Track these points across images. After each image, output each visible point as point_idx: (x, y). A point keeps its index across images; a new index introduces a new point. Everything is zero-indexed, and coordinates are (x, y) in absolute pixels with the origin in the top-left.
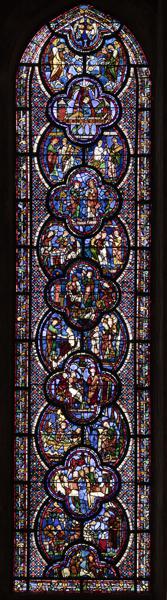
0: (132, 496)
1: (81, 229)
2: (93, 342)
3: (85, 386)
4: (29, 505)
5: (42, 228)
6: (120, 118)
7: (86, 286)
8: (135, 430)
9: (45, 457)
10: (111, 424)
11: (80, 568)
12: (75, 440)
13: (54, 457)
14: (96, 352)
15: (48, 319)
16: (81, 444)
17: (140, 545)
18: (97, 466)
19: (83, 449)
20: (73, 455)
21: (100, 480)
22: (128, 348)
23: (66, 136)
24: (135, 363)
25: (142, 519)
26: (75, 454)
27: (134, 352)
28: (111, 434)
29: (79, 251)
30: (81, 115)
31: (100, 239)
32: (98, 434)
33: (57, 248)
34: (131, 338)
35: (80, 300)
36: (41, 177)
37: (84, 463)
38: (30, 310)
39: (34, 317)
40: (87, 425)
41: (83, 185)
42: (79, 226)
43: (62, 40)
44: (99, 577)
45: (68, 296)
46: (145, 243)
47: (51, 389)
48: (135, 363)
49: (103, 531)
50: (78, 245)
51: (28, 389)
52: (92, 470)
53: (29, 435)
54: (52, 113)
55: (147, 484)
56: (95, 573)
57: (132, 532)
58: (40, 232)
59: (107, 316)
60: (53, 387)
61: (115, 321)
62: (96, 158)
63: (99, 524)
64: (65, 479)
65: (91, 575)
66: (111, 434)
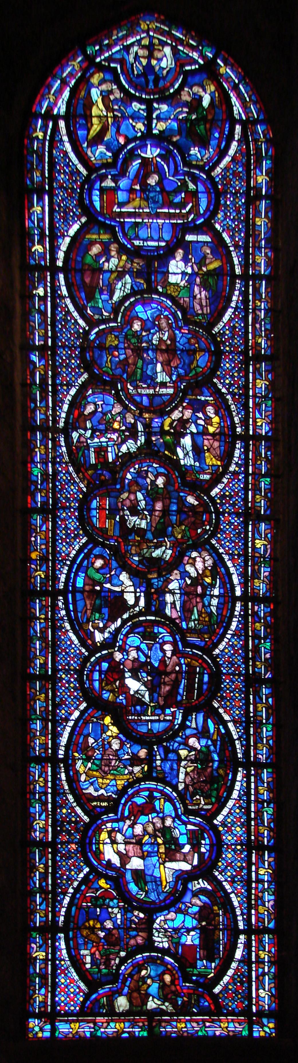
0: (242, 868)
1: (145, 401)
2: (169, 598)
3: (156, 675)
4: (55, 886)
5: (74, 397)
6: (214, 214)
7: (154, 500)
8: (246, 753)
9: (83, 800)
10: (203, 742)
11: (148, 995)
12: (137, 769)
13: (100, 798)
14: (174, 615)
15: (87, 557)
16: (147, 777)
17: (257, 956)
18: (178, 816)
19: (152, 785)
20: (133, 796)
21: (183, 840)
22: (233, 609)
23: (117, 241)
25: (261, 909)
26: (137, 793)
27: (245, 616)
28: (202, 758)
29: (142, 439)
30: (144, 203)
31: (181, 420)
32: (179, 759)
33: (102, 435)
34: (238, 593)
35: (143, 524)
36: (71, 308)
37: (154, 810)
38: (54, 541)
39: (62, 549)
40: (159, 743)
41: (149, 325)
42: (141, 395)
43: (108, 77)
44: (183, 1011)
45: (122, 518)
46: (264, 430)
47: (92, 681)
48: (247, 636)
49: (188, 930)
50: (140, 427)
51: (51, 680)
52: (169, 822)
53: (54, 761)
54: (91, 201)
55: (270, 849)
56: (174, 1004)
57: (242, 932)
58: (71, 405)
59: (194, 554)
60: (96, 676)
61: (210, 562)
62: (173, 279)
63: (180, 917)
64: (119, 837)
65: (167, 1007)
66: (202, 758)
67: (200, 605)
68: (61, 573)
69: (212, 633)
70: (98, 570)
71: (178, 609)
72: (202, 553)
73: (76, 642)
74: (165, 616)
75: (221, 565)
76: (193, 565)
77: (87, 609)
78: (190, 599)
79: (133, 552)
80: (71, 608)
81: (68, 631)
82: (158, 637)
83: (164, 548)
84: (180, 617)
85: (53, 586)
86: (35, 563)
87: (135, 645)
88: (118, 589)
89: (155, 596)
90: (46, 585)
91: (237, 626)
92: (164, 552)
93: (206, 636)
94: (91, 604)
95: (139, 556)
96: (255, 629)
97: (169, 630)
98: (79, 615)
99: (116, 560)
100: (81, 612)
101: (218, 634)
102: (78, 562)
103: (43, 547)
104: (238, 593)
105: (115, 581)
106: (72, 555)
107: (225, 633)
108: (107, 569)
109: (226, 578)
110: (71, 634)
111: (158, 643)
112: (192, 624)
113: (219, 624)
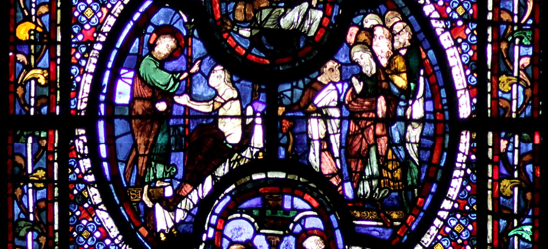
2: (316, 128)
14: (328, 167)
15: (138, 31)
22: (454, 150)
24: (482, 212)
27: (478, 165)
34: (465, 110)
48: (482, 212)
59: (371, 20)
61: (404, 38)
67: (383, 142)
68: (83, 71)
69: (407, 206)
70: (161, 64)
71: (337, 154)
72: (389, 15)
73: (114, 232)
74: (307, 170)
75: (427, 44)
76: (368, 46)
77: (138, 155)
78: (363, 130)
79: (240, 17)
80: (104, 154)
81: (95, 207)
82: (291, 220)
83: (305, 5)
84: (339, 173)
85: (65, 103)
86: (25, 50)
87: (243, 239)
88: (204, 108)
89: (286, 124)
90: (50, 103)
91: (463, 188)
92: (306, 16)
93: (395, 216)
94: (146, 144)
95: (252, 28)
96: (500, 194)
97: (315, 203)
98: (121, 168)
99: (201, 38)
100: (126, 162)
101: (421, 209)
102: (118, 46)
103: (44, 10)
104: (465, 110)
105: (199, 89)
106: (106, 29)
107: (436, 206)
108: (183, 59)
109: (439, 75)
110: (103, 215)
111: (291, 233)
112: (365, 188)
113: (423, 187)
